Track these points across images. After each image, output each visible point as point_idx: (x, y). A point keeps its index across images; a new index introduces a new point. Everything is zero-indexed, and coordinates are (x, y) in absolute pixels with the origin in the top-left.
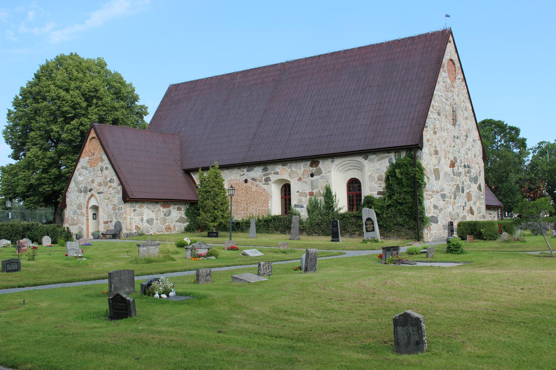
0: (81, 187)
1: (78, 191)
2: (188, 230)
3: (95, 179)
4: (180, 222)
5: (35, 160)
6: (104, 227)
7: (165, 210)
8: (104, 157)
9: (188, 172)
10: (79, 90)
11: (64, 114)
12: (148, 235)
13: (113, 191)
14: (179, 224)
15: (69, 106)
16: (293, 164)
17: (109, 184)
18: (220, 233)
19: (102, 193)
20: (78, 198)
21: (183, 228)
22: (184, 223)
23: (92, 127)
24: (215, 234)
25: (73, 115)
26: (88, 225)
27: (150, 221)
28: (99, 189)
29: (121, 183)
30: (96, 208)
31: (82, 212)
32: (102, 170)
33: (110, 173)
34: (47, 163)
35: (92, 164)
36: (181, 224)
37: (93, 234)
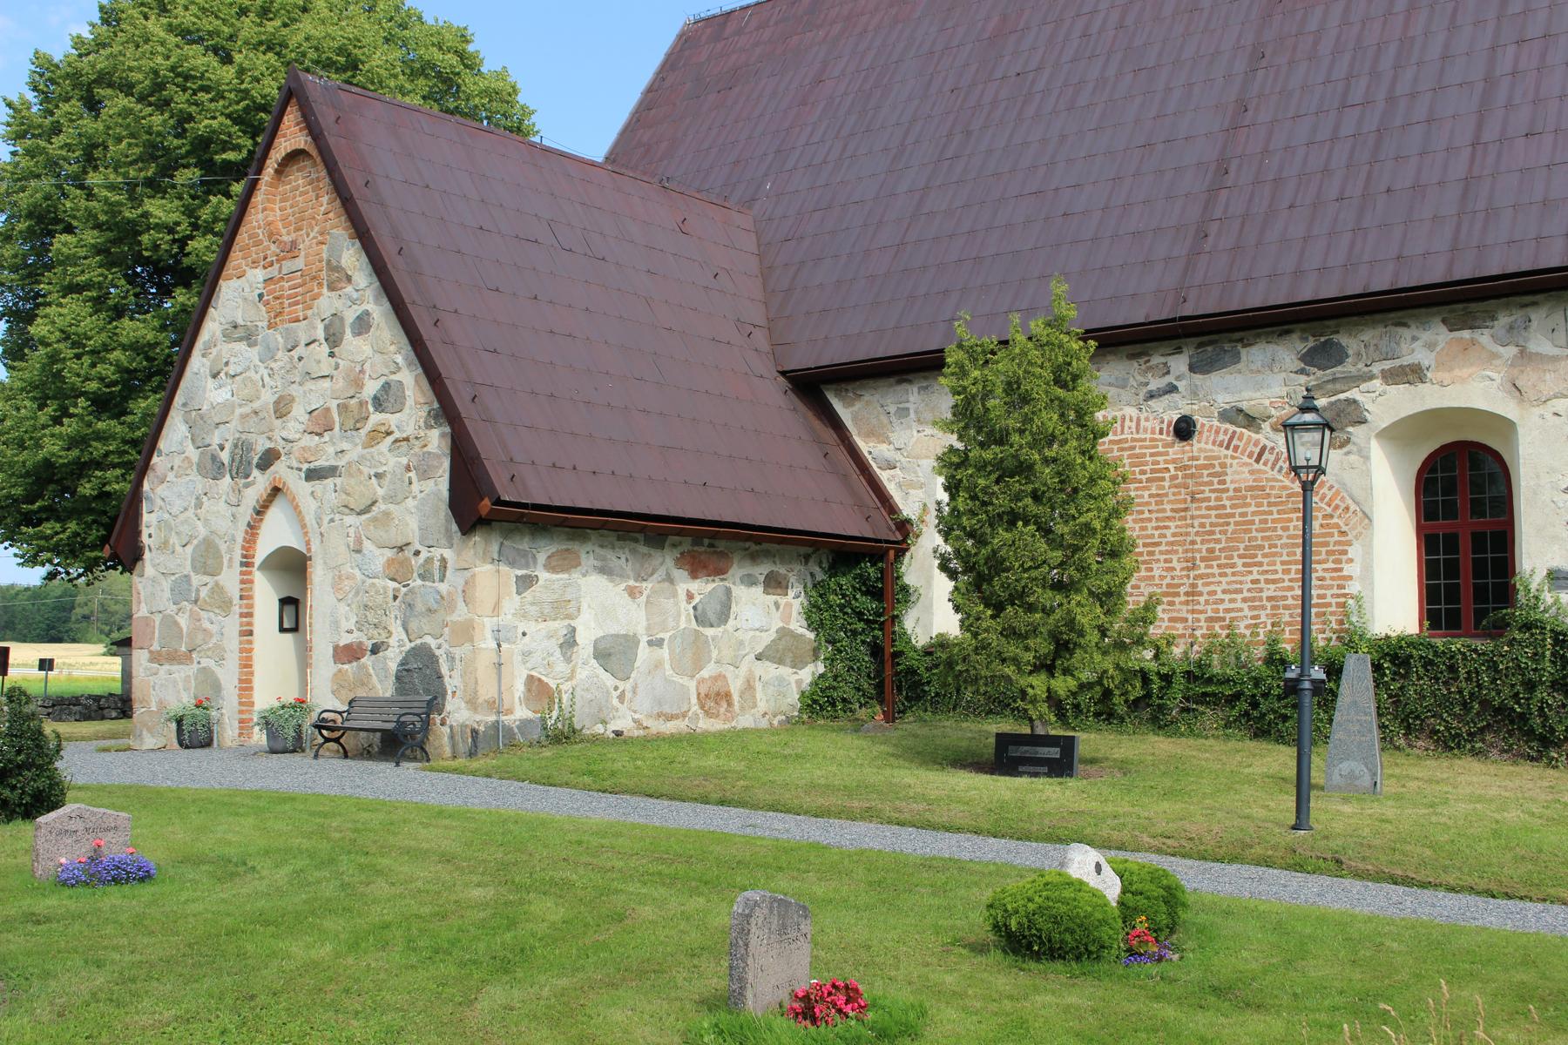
0: (216, 440)
1: (201, 469)
2: (821, 704)
3: (295, 390)
4: (780, 662)
5: (70, 353)
6: (339, 682)
7: (702, 587)
8: (352, 257)
9: (811, 387)
10: (278, 54)
11: (203, 147)
12: (596, 740)
13: (390, 460)
14: (769, 670)
15: (228, 116)
16: (1538, 316)
17: (376, 418)
18: (1089, 741)
19: (331, 471)
20: (199, 505)
21: (793, 697)
22: (797, 664)
23: (291, 94)
24: (1054, 753)
25: (244, 153)
26: (247, 664)
27: (614, 654)
28: (317, 450)
29: (447, 410)
30: (292, 565)
31: (218, 589)
32: (333, 339)
33: (380, 352)
34: (121, 369)
35: (280, 305)
36: (785, 671)
37: (267, 723)
